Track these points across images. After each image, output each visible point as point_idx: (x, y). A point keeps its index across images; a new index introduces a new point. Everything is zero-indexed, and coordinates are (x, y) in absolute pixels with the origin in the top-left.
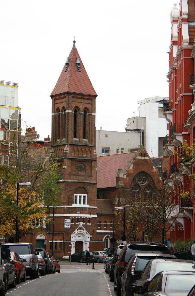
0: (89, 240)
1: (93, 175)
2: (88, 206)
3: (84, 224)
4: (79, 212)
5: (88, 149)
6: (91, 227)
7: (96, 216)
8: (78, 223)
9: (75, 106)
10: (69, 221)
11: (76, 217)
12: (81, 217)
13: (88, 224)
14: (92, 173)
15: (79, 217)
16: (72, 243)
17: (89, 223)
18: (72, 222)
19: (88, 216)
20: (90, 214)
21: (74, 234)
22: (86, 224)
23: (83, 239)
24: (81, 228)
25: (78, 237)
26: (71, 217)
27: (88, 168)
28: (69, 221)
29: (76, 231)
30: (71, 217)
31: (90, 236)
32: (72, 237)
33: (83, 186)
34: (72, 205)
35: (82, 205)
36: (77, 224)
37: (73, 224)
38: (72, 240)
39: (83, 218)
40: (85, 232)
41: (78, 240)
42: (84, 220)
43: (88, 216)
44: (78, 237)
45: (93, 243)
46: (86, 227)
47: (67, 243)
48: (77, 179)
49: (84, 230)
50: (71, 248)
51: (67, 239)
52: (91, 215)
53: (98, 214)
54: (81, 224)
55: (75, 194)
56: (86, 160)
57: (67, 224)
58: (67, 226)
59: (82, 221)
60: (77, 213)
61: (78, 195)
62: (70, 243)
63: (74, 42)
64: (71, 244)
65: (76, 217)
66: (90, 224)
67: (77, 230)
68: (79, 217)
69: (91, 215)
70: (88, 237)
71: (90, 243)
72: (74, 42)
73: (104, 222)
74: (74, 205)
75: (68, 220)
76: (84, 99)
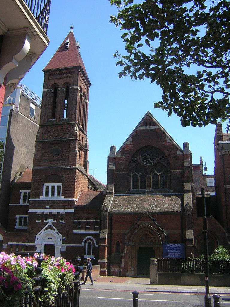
1: (70, 158)
2: (62, 198)
4: (49, 207)
9: (52, 84)
13: (60, 221)
14: (70, 155)
19: (62, 211)
21: (40, 234)
22: (58, 222)
24: (50, 227)
35: (50, 198)
36: (45, 221)
42: (51, 215)
43: (62, 211)
46: (58, 226)
49: (54, 230)
52: (65, 209)
54: (50, 221)
60: (46, 208)
61: (50, 185)
65: (45, 213)
67: (45, 230)
68: (49, 213)
76: (64, 73)
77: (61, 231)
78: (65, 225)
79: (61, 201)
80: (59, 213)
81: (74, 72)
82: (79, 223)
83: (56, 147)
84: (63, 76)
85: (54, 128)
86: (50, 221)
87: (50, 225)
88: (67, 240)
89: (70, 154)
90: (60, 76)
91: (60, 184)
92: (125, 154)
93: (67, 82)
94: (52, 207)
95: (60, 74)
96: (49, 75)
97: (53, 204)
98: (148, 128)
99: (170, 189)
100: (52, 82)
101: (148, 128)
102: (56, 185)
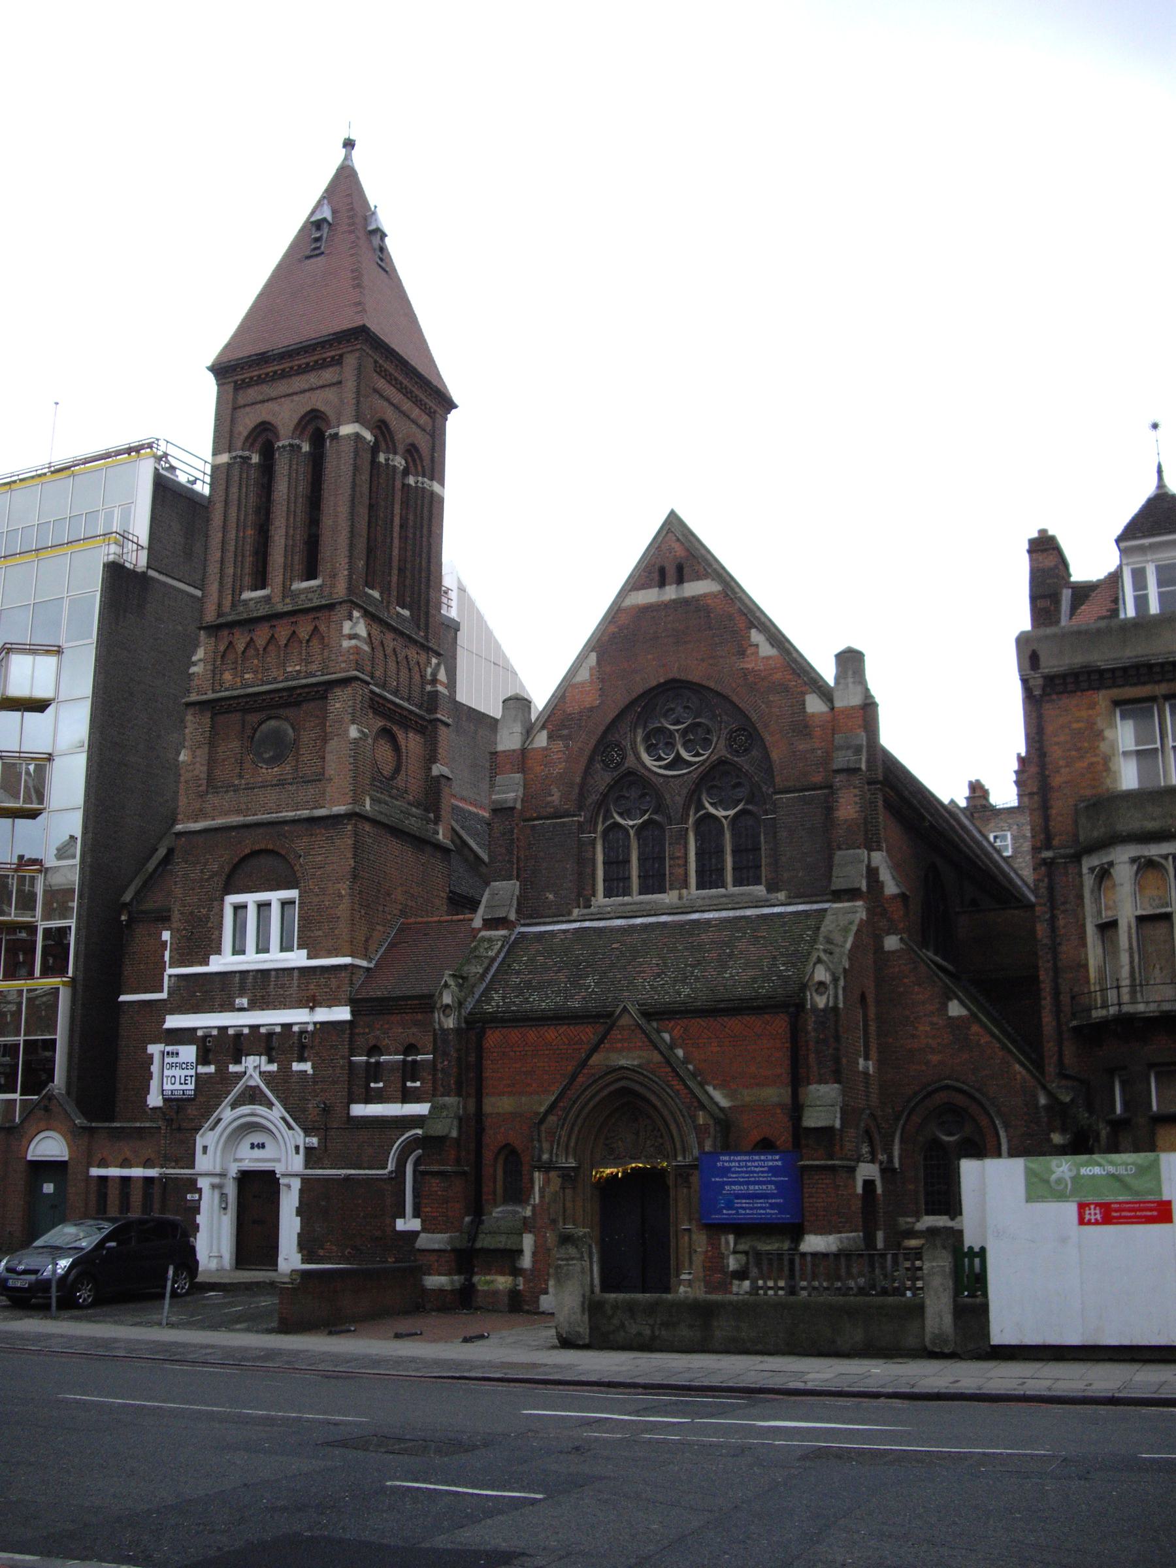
0: (297, 1163)
2: (298, 958)
3: (273, 1067)
5: (310, 628)
6: (315, 1083)
7: (342, 1014)
8: (238, 1062)
9: (251, 425)
10: (188, 1053)
11: (231, 1032)
12: (254, 1028)
13: (296, 1066)
14: (328, 757)
15: (246, 1031)
16: (203, 1183)
17: (302, 1059)
18: (203, 1059)
19: (298, 1016)
20: (312, 1003)
21: (212, 1129)
22: (285, 1069)
23: (279, 1160)
24: (252, 1096)
25: (253, 1146)
26: (200, 1033)
27: (307, 737)
28: (188, 1053)
29: (227, 1115)
30: (200, 1033)
31: (298, 1137)
32: (205, 1148)
33: (270, 847)
34: (207, 964)
35: (251, 960)
36: (233, 1068)
37: (212, 1069)
38: (203, 1163)
39: (270, 1035)
40: (275, 1114)
41: (247, 1165)
43: (298, 1016)
44: (253, 1146)
45: (327, 1180)
46: (281, 1083)
47: (176, 1180)
48: (239, 812)
49: (270, 1105)
50: (197, 1210)
51: (177, 1161)
52: (312, 1009)
53: (356, 1005)
55: (232, 899)
56: (295, 688)
57: (177, 1072)
58: (177, 1086)
59: (261, 1050)
61: (251, 899)
62: (191, 1185)
63: (349, 144)
64: (200, 1191)
65: (231, 1032)
66: (307, 1067)
67: (234, 1106)
68: (246, 1031)
69: (312, 1009)
70: (297, 1148)
71: (307, 1182)
72: (349, 144)
73: (401, 1048)
74: (218, 964)
75: (182, 1049)
77: (298, 1114)
78: (315, 1083)
79: (296, 973)
80: (287, 1027)
81: (341, 356)
82: (375, 1071)
83: (273, 723)
84: (298, 383)
85: (261, 635)
86: (254, 1067)
87: (252, 1083)
88: (326, 1150)
89: (329, 748)
90: (282, 387)
91: (293, 894)
92: (565, 732)
93: (313, 411)
94: (258, 1004)
95: (284, 375)
96: (239, 387)
97: (263, 987)
98: (671, 593)
99: (772, 888)
100: (248, 421)
101: (671, 593)
102: (275, 897)
